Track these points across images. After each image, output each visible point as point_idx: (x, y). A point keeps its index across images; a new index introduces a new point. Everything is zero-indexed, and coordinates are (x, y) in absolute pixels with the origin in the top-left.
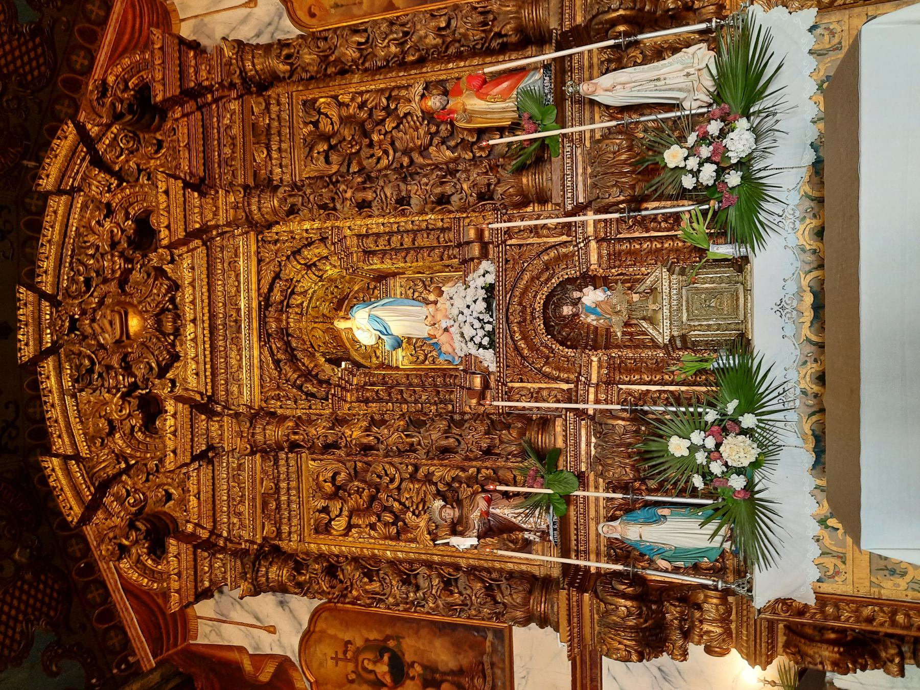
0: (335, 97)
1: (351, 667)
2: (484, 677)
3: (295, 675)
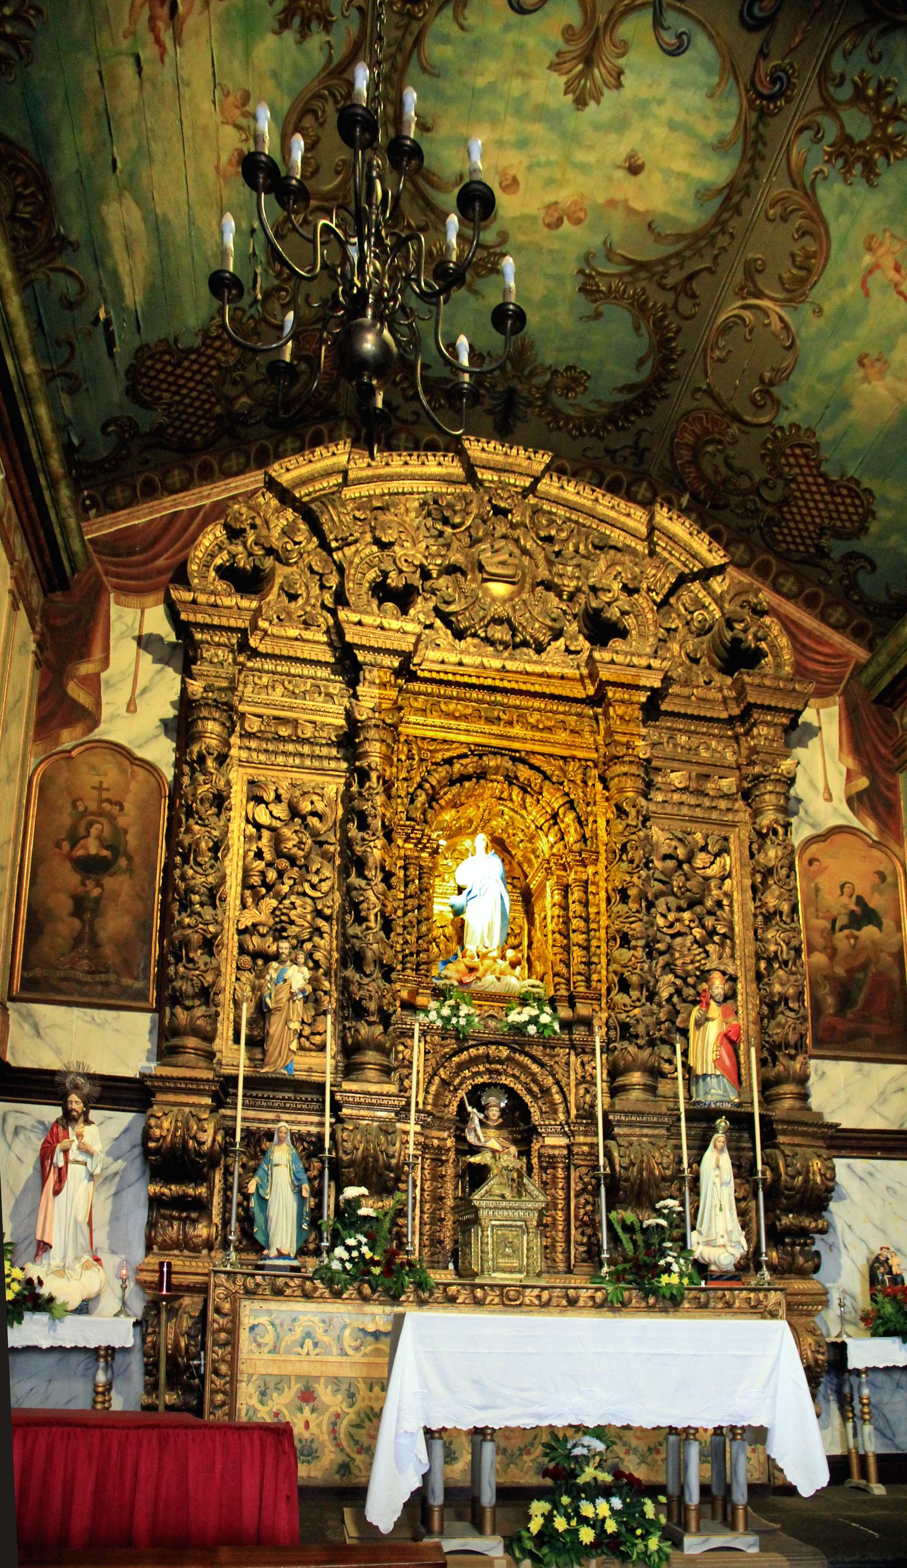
0: (729, 876)
1: (93, 806)
2: (91, 973)
3: (79, 729)
